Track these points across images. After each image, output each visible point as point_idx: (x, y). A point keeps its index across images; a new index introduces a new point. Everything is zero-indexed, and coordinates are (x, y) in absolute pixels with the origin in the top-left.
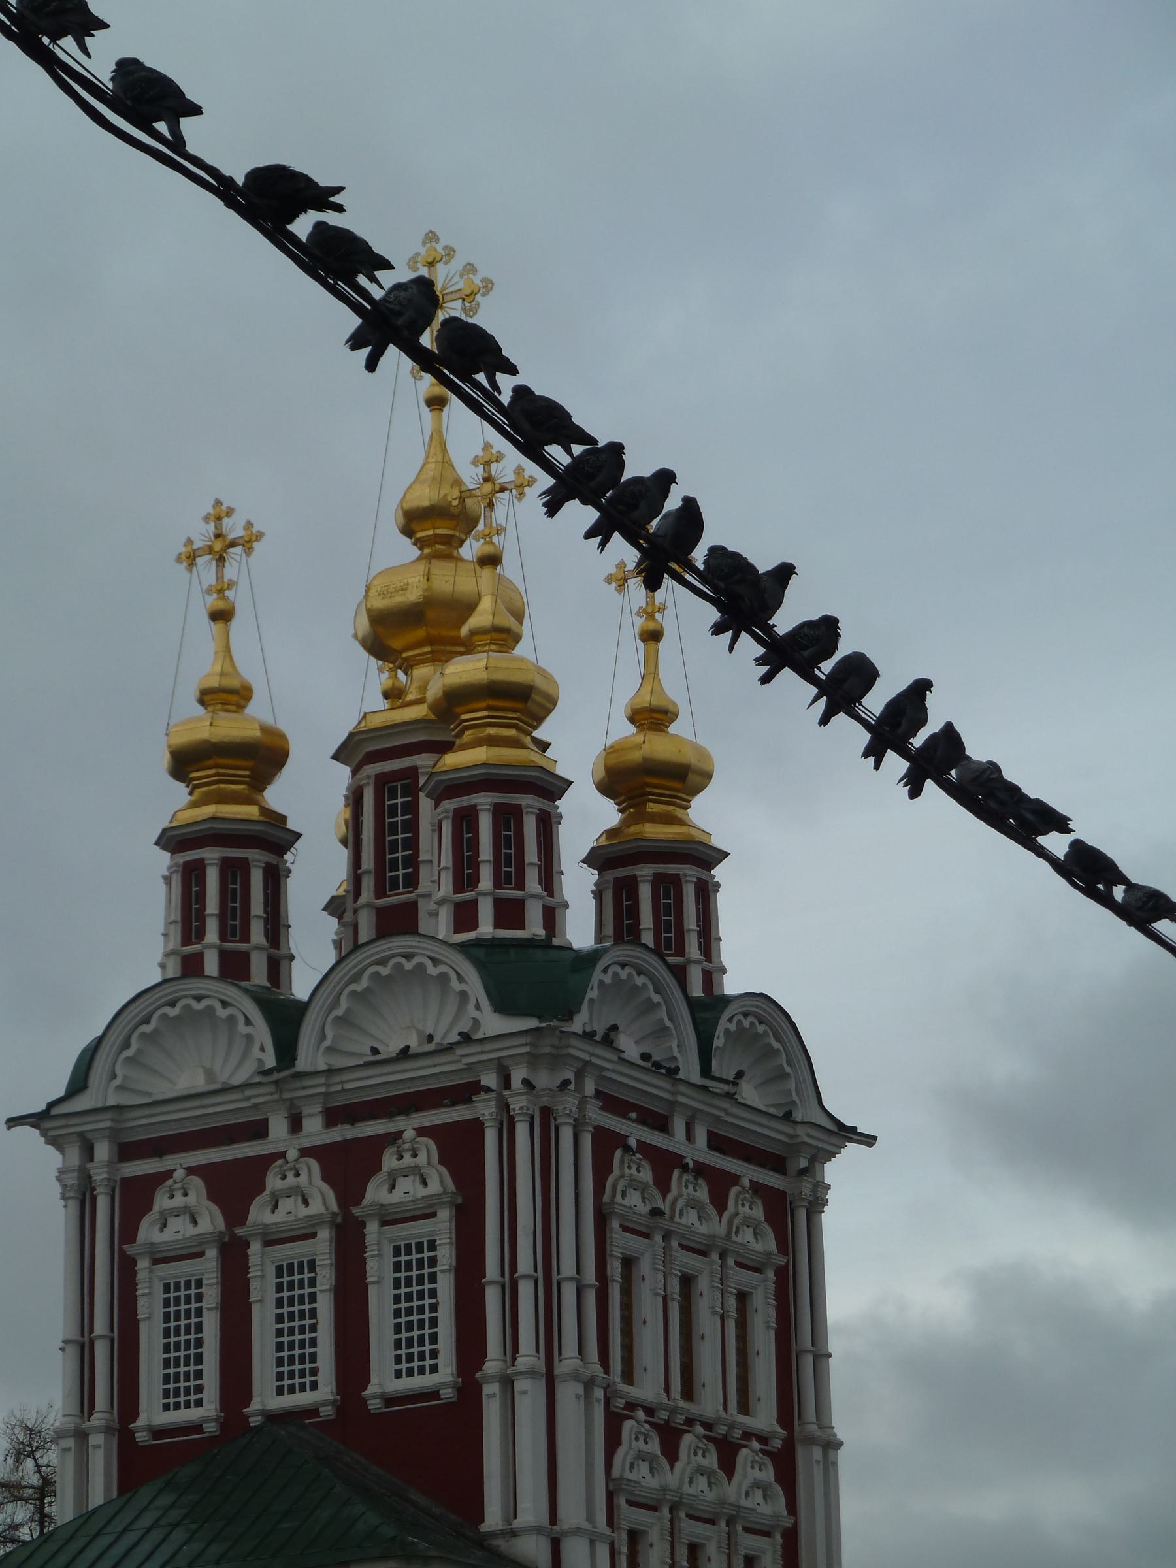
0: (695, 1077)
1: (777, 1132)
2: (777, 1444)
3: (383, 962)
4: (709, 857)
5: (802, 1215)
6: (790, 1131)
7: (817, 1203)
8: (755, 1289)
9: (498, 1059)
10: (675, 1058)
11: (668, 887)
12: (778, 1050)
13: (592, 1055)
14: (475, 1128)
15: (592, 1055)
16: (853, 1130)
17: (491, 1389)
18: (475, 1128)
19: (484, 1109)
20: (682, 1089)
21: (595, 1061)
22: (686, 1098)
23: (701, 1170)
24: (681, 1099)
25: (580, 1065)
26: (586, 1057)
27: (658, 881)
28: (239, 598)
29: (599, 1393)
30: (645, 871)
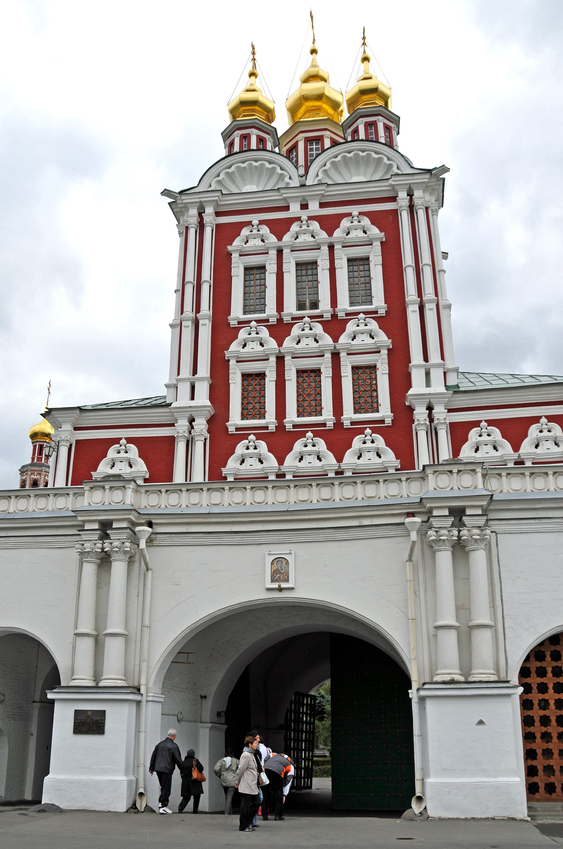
1: (381, 189)
2: (382, 312)
6: (387, 184)
8: (370, 253)
10: (288, 183)
12: (380, 158)
13: (200, 198)
15: (200, 198)
16: (435, 168)
20: (282, 191)
21: (202, 200)
22: (287, 194)
23: (310, 218)
24: (284, 196)
25: (198, 205)
26: (198, 200)
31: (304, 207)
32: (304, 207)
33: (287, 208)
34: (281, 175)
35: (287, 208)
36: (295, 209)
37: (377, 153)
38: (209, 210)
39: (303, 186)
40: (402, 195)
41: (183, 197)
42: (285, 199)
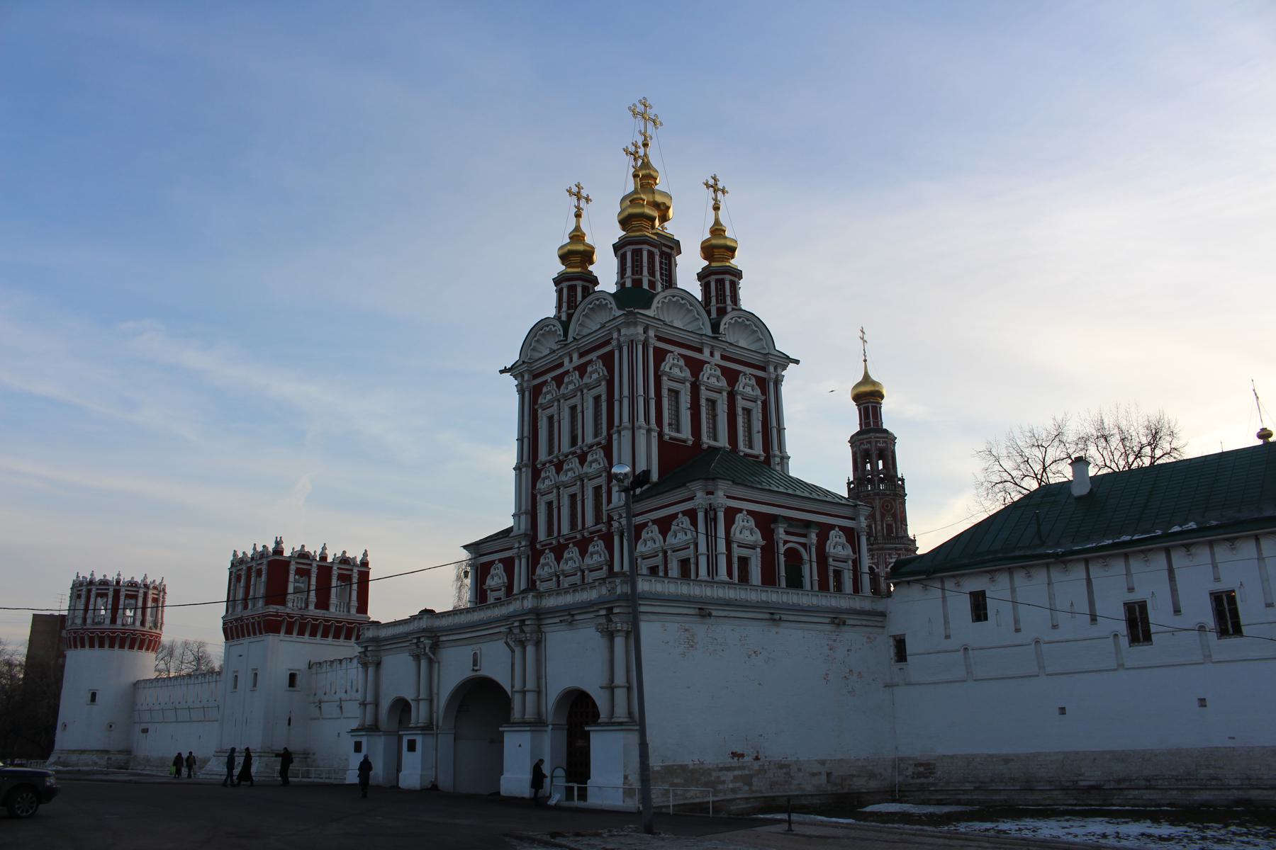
0: (709, 333)
1: (756, 359)
3: (591, 303)
4: (738, 274)
5: (772, 385)
7: (778, 382)
9: (616, 326)
11: (720, 283)
12: (757, 331)
14: (612, 352)
17: (615, 437)
18: (612, 352)
19: (614, 343)
20: (704, 338)
22: (705, 340)
27: (717, 281)
28: (584, 214)
29: (655, 434)
30: (714, 277)
31: (712, 354)
32: (712, 354)
33: (700, 351)
34: (698, 319)
35: (700, 351)
36: (707, 351)
37: (756, 326)
38: (651, 333)
39: (716, 338)
40: (772, 369)
41: (639, 316)
42: (703, 343)
